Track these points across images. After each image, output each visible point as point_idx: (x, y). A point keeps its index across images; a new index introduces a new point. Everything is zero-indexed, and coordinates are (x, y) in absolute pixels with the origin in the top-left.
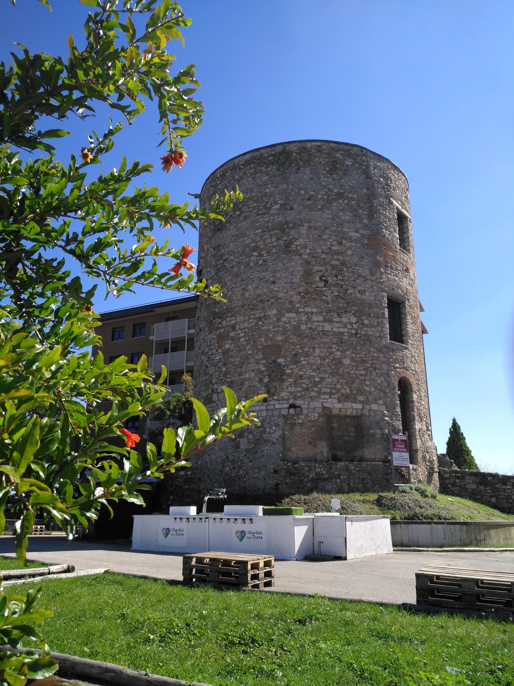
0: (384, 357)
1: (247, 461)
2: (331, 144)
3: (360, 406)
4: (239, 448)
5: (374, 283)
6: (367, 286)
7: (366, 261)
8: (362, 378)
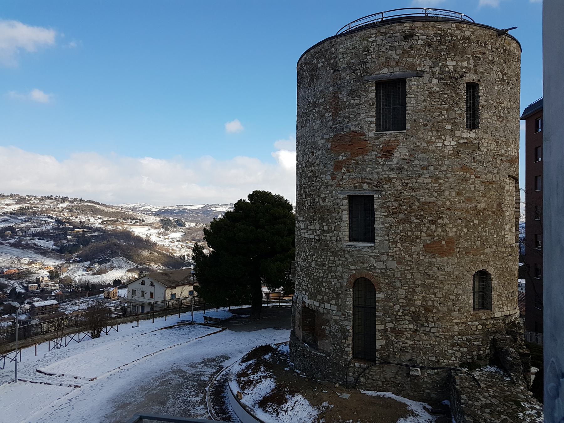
0: (339, 260)
2: (311, 51)
3: (317, 304)
5: (333, 188)
6: (328, 192)
7: (329, 166)
8: (320, 280)
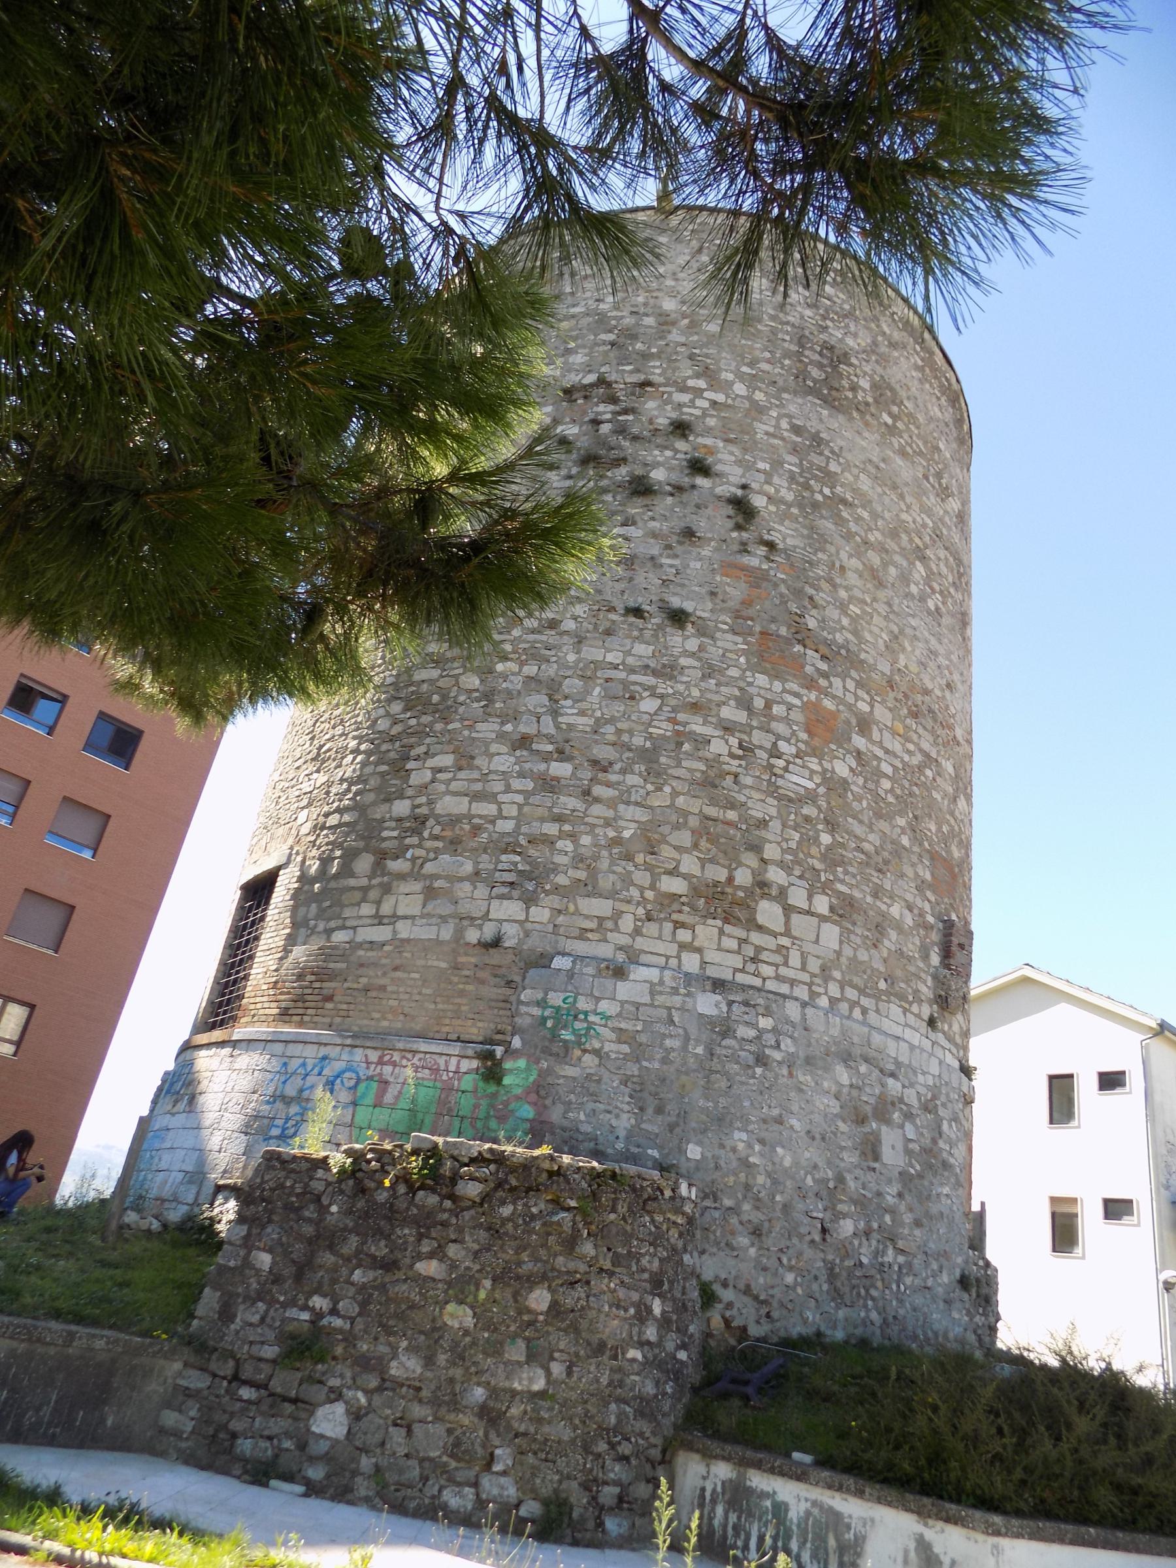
1: (908, 1218)
4: (877, 1157)
